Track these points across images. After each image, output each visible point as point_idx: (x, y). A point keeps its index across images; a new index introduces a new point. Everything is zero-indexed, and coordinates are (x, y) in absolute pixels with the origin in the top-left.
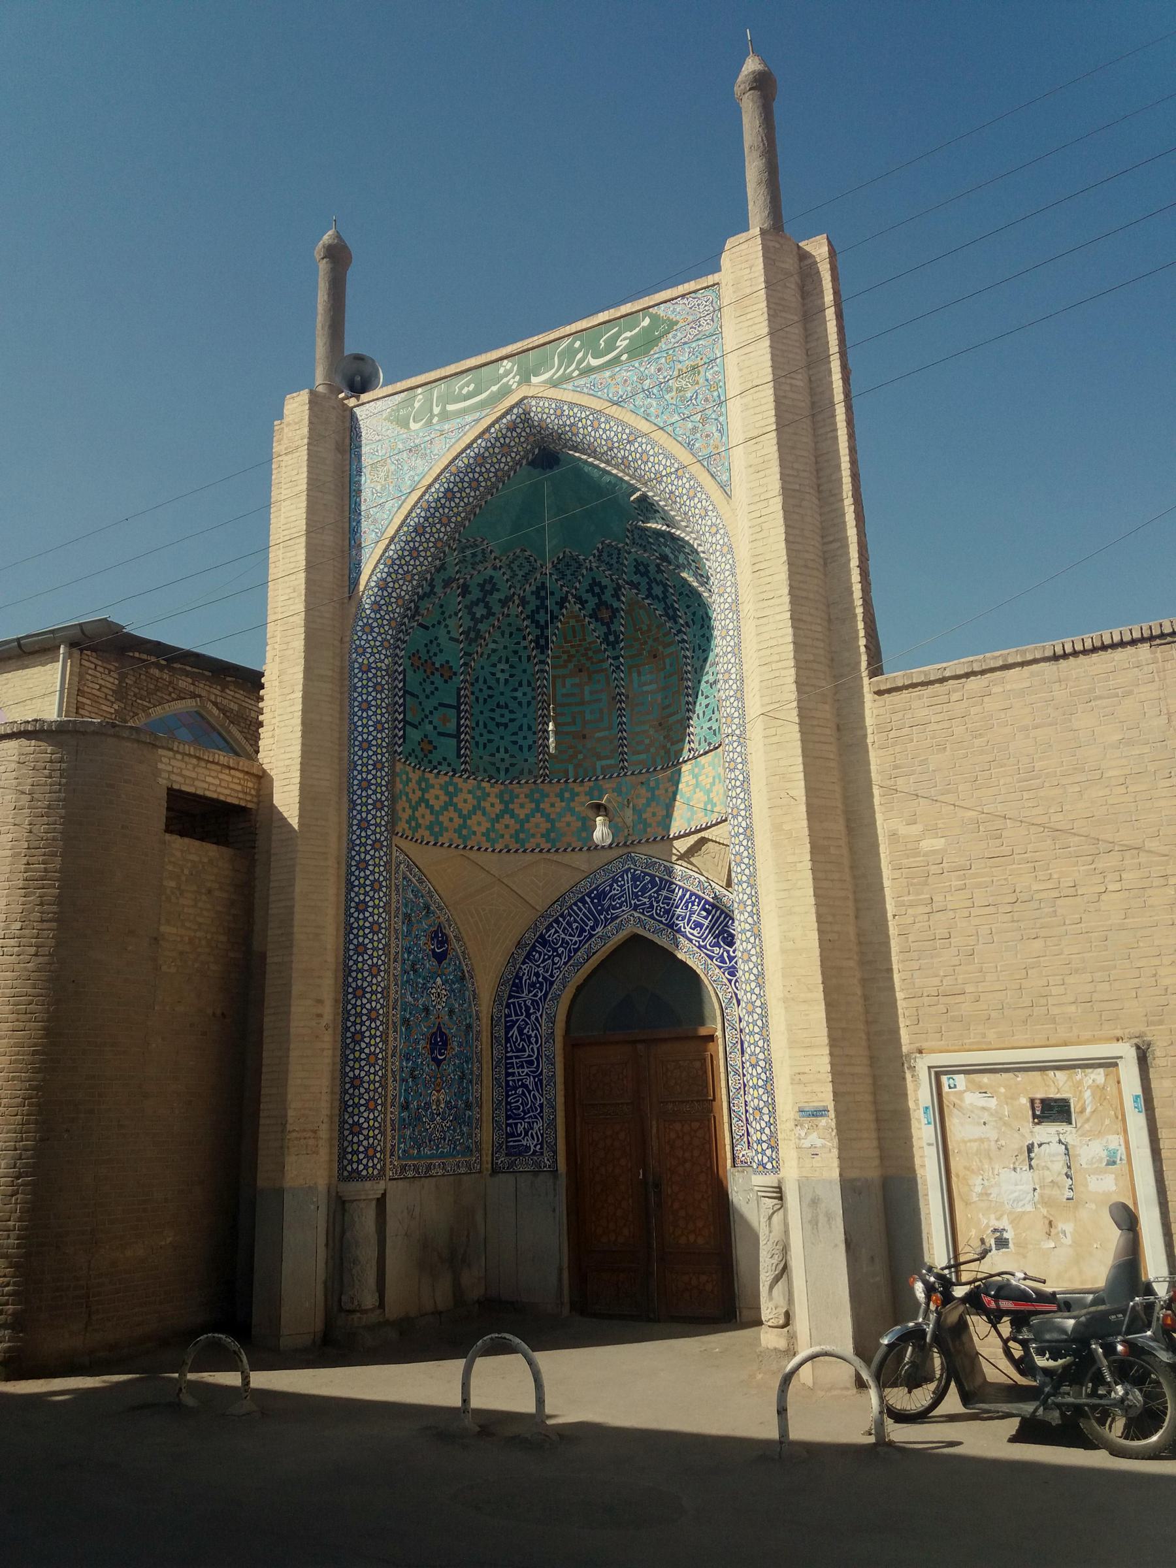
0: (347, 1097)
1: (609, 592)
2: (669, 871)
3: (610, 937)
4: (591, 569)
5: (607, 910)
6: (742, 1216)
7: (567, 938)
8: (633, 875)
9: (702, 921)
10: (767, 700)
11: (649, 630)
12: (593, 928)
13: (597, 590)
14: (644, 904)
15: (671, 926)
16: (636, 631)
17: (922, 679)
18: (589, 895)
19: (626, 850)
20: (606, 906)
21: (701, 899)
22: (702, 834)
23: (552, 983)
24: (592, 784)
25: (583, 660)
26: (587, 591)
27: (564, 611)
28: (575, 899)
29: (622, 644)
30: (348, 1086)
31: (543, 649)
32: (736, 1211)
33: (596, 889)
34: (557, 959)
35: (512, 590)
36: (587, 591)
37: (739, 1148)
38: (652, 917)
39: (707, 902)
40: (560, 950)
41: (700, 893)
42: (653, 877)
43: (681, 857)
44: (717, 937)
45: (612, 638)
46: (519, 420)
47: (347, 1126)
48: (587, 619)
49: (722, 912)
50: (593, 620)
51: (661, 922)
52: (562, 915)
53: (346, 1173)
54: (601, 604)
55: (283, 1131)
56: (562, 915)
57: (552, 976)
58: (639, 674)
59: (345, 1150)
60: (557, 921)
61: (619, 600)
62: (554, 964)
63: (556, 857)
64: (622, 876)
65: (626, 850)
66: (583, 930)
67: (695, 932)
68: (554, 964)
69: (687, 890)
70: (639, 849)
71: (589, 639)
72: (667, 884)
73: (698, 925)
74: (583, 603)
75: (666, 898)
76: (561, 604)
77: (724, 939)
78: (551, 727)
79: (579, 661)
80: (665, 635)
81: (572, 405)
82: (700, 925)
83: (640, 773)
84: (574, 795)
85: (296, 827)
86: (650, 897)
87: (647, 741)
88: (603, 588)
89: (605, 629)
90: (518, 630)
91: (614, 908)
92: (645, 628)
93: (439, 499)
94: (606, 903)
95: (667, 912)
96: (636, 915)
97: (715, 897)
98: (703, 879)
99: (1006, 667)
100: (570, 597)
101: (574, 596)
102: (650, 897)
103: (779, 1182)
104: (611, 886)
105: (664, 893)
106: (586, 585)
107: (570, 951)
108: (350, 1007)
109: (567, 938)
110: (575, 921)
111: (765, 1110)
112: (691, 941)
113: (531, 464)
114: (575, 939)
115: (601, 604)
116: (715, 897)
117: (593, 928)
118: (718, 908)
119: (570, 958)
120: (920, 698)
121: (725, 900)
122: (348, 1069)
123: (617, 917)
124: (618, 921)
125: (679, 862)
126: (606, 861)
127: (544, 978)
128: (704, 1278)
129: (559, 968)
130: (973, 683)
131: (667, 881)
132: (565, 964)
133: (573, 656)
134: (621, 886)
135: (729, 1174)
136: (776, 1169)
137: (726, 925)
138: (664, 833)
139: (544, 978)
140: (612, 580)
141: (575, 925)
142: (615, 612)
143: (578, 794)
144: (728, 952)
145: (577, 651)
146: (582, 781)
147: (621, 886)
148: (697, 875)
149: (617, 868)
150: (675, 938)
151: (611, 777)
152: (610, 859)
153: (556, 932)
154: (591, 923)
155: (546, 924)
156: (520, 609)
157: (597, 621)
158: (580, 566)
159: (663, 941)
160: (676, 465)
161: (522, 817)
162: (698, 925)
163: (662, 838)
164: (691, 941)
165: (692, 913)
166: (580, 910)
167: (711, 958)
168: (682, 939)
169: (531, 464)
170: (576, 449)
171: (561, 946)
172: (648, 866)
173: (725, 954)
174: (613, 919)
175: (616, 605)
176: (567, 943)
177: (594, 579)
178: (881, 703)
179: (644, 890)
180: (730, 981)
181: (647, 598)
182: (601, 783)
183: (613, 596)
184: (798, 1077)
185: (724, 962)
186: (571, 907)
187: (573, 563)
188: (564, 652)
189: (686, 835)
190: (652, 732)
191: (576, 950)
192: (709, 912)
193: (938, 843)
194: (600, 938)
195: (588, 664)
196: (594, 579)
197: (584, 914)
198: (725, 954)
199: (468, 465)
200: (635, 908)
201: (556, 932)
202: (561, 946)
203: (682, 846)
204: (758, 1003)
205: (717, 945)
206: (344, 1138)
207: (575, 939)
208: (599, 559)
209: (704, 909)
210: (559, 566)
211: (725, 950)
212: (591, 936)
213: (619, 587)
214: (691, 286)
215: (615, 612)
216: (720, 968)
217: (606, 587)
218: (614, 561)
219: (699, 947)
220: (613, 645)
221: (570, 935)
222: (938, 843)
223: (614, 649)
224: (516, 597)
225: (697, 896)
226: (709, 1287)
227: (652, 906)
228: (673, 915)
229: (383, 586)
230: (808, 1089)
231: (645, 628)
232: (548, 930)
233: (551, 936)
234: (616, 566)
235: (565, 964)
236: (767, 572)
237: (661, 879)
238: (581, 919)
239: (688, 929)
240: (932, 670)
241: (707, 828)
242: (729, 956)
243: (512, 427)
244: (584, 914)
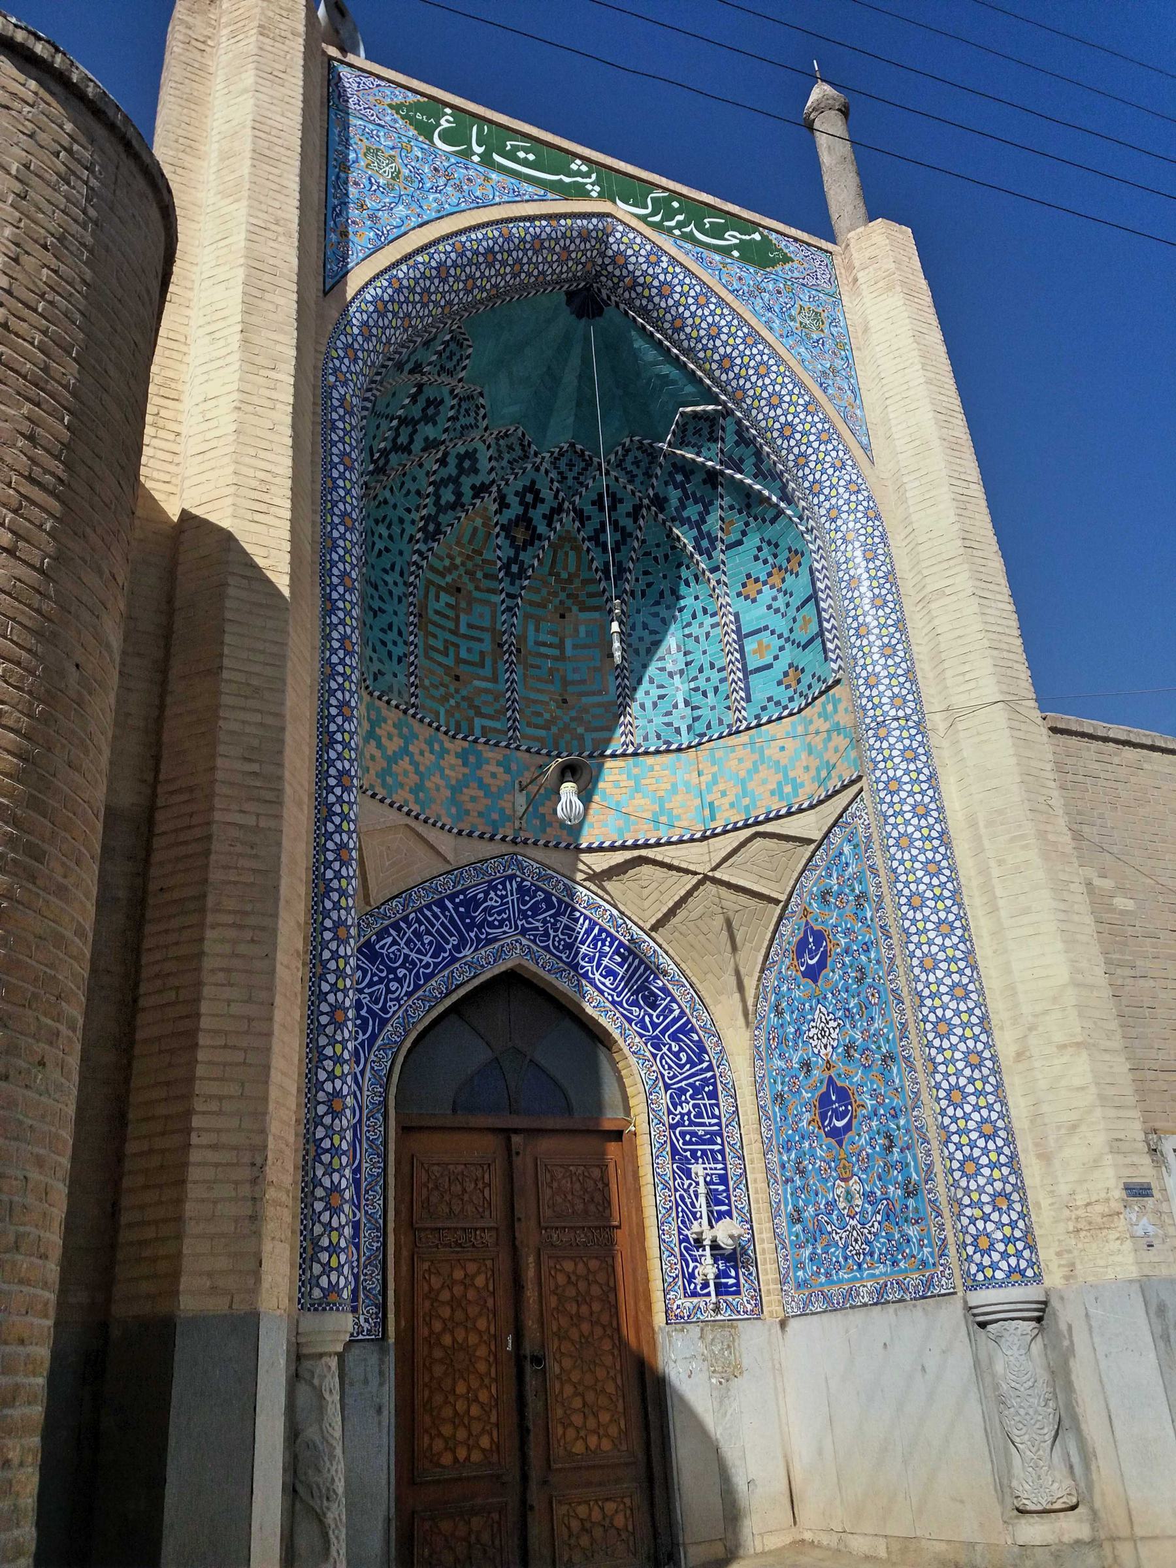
0: (320, 1132)
1: (543, 509)
2: (572, 894)
3: (481, 963)
4: (537, 469)
5: (480, 927)
6: (681, 1399)
7: (413, 955)
8: (520, 886)
9: (616, 968)
10: (1004, 688)
11: (570, 580)
12: (457, 948)
13: (529, 498)
14: (536, 929)
15: (575, 967)
16: (550, 574)
17: (1091, 731)
18: (451, 898)
19: (512, 849)
20: (478, 920)
21: (614, 939)
22: (644, 852)
23: (384, 1023)
24: (466, 744)
25: (466, 579)
26: (517, 494)
27: (478, 501)
28: (428, 900)
29: (526, 583)
30: (321, 1109)
31: (432, 536)
32: (675, 1391)
33: (463, 892)
34: (394, 986)
35: (445, 436)
36: (517, 494)
37: (671, 1295)
38: (547, 949)
39: (621, 944)
40: (401, 972)
41: (612, 931)
42: (549, 895)
43: (590, 878)
44: (636, 993)
45: (515, 569)
46: (594, 234)
47: (320, 1193)
48: (497, 529)
49: (642, 962)
50: (503, 534)
51: (560, 958)
52: (405, 919)
53: (317, 1293)
54: (524, 520)
55: (254, 1181)
56: (405, 919)
57: (384, 1010)
58: (537, 630)
59: (315, 1241)
60: (395, 926)
61: (549, 525)
62: (389, 991)
63: (421, 829)
64: (503, 884)
65: (512, 849)
66: (440, 949)
67: (607, 982)
68: (389, 991)
69: (596, 924)
70: (531, 851)
71: (487, 555)
72: (566, 907)
73: (610, 973)
74: (503, 504)
75: (566, 927)
76: (479, 491)
77: (644, 998)
78: (615, 627)
79: (460, 576)
80: (591, 595)
81: (674, 261)
82: (614, 974)
83: (538, 753)
84: (445, 750)
85: (286, 592)
86: (545, 921)
87: (547, 716)
88: (538, 499)
89: (512, 553)
90: (418, 493)
91: (491, 925)
92: (564, 575)
93: (476, 253)
94: (478, 916)
95: (569, 947)
96: (524, 942)
97: (631, 940)
98: (615, 912)
99: (1153, 748)
100: (494, 489)
101: (499, 490)
102: (545, 921)
103: (1047, 1295)
104: (486, 893)
105: (564, 920)
106: (519, 485)
107: (417, 975)
108: (326, 955)
109: (413, 955)
110: (429, 933)
111: (1015, 1197)
112: (602, 992)
113: (570, 295)
114: (427, 959)
115: (524, 520)
116: (631, 940)
117: (457, 948)
118: (636, 956)
119: (417, 987)
120: (1089, 749)
121: (644, 946)
122: (322, 1075)
123: (495, 940)
124: (496, 945)
125: (587, 884)
126: (481, 857)
127: (370, 1010)
128: (610, 1507)
129: (397, 999)
130: (1129, 753)
131: (568, 905)
132: (409, 994)
133: (456, 567)
134: (502, 897)
135: (660, 1338)
136: (1038, 1278)
137: (647, 980)
138: (570, 840)
139: (370, 1010)
140: (556, 497)
141: (427, 939)
142: (534, 537)
143: (448, 752)
144: (651, 1016)
145: (463, 564)
146: (454, 737)
147: (502, 897)
148: (608, 907)
149: (495, 870)
150: (579, 985)
151: (496, 745)
152: (488, 856)
153: (394, 943)
154: (454, 941)
155: (377, 927)
156: (435, 467)
157: (506, 537)
158: (526, 457)
159: (564, 985)
160: (807, 398)
161: (390, 752)
162: (610, 973)
163: (567, 847)
164: (602, 992)
165: (603, 955)
166: (437, 918)
167: (630, 1021)
168: (589, 988)
169: (570, 295)
170: (644, 312)
171: (403, 966)
172: (540, 877)
173: (647, 1019)
174: (489, 942)
175: (542, 529)
176: (413, 963)
177: (533, 482)
178: (1054, 741)
179: (535, 910)
180: (654, 1056)
181: (590, 539)
182: (480, 747)
183: (544, 516)
184: (1115, 1144)
185: (644, 1028)
186: (420, 910)
187: (517, 447)
188: (449, 556)
189: (613, 848)
190: (553, 706)
191: (428, 977)
192: (625, 959)
193: (1130, 905)
194: (470, 965)
195: (471, 587)
196: (533, 482)
197: (442, 924)
198: (647, 1019)
199: (523, 240)
200: (524, 931)
201: (394, 943)
202: (403, 966)
203: (600, 862)
204: (987, 1054)
205: (635, 1003)
206: (316, 1217)
207: (427, 959)
208: (555, 462)
209: (617, 952)
210: (501, 442)
211: (646, 1013)
212: (454, 960)
213: (559, 510)
214: (805, 236)
215: (534, 537)
216: (641, 1036)
217: (543, 501)
218: (570, 475)
219: (613, 1003)
220: (513, 578)
221: (419, 952)
222: (1130, 905)
223: (512, 583)
224: (443, 448)
225: (609, 934)
226: (619, 1521)
227: (546, 934)
228: (577, 953)
229: (381, 308)
230: (1128, 1160)
231: (564, 575)
232: (381, 935)
233: (385, 946)
234: (570, 482)
235: (409, 994)
236: (980, 553)
237: (560, 901)
238: (438, 931)
239: (597, 976)
240: (1088, 726)
241: (658, 844)
242: (652, 1022)
243: (585, 236)
244: (442, 924)
